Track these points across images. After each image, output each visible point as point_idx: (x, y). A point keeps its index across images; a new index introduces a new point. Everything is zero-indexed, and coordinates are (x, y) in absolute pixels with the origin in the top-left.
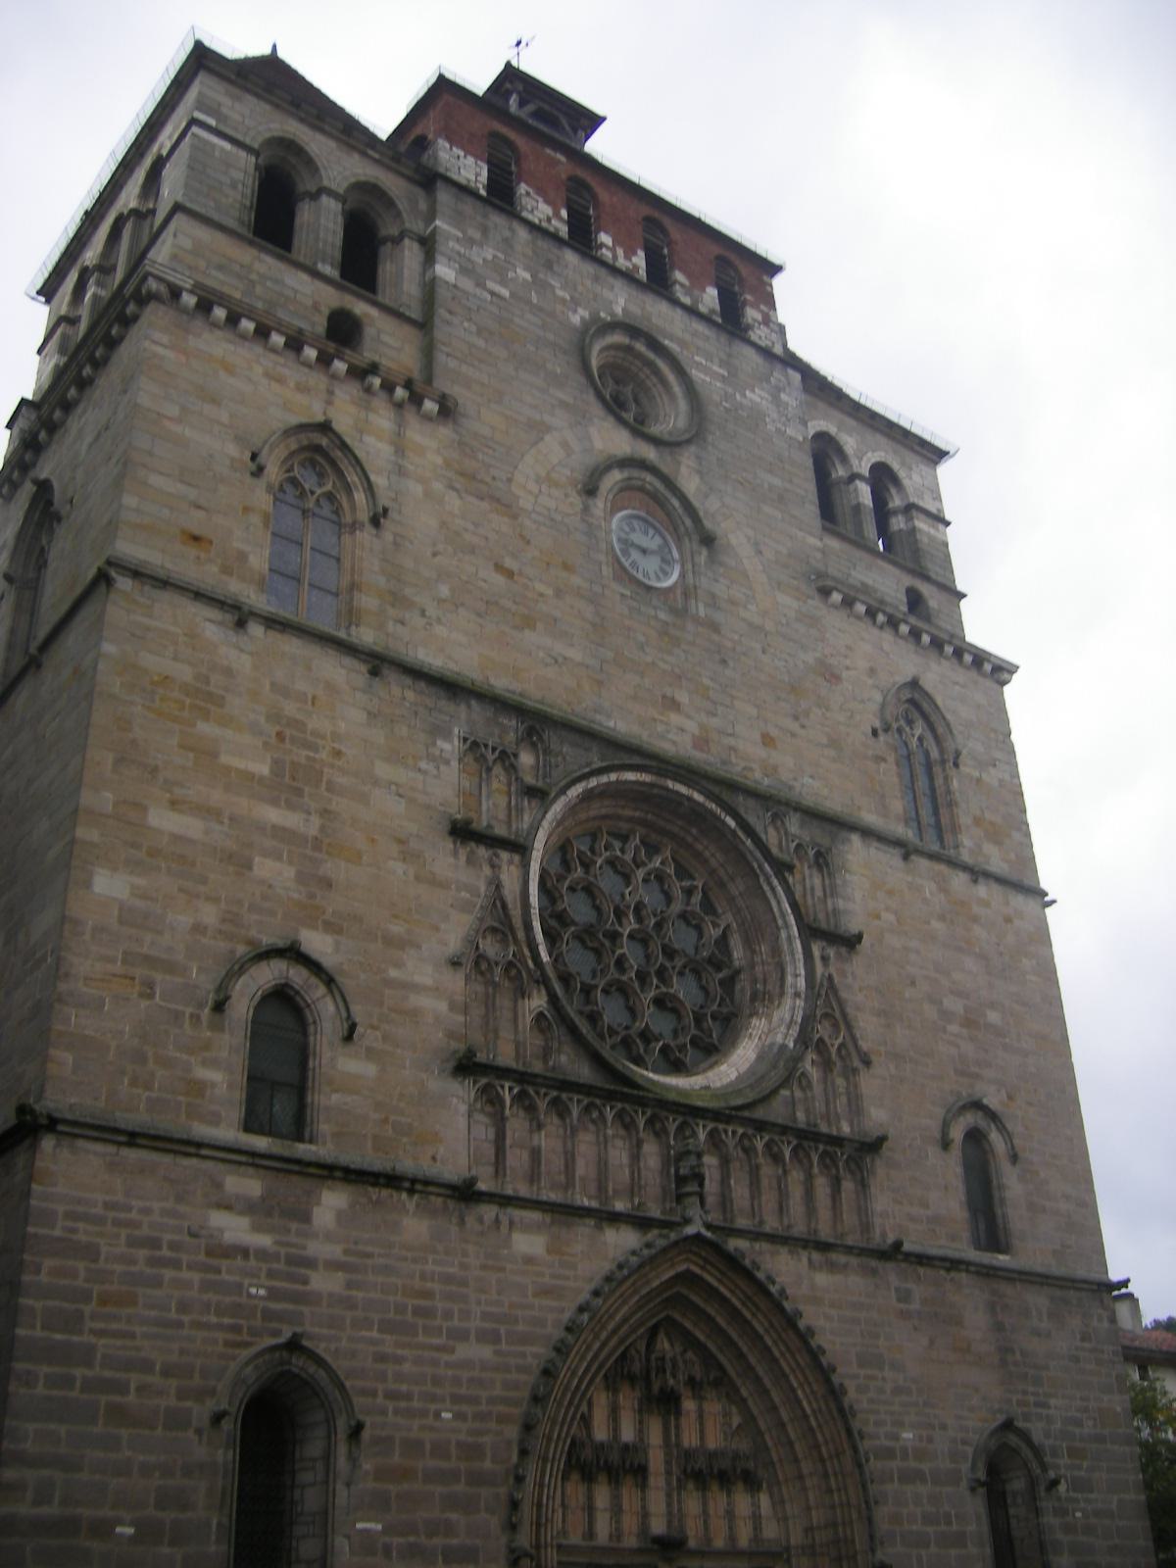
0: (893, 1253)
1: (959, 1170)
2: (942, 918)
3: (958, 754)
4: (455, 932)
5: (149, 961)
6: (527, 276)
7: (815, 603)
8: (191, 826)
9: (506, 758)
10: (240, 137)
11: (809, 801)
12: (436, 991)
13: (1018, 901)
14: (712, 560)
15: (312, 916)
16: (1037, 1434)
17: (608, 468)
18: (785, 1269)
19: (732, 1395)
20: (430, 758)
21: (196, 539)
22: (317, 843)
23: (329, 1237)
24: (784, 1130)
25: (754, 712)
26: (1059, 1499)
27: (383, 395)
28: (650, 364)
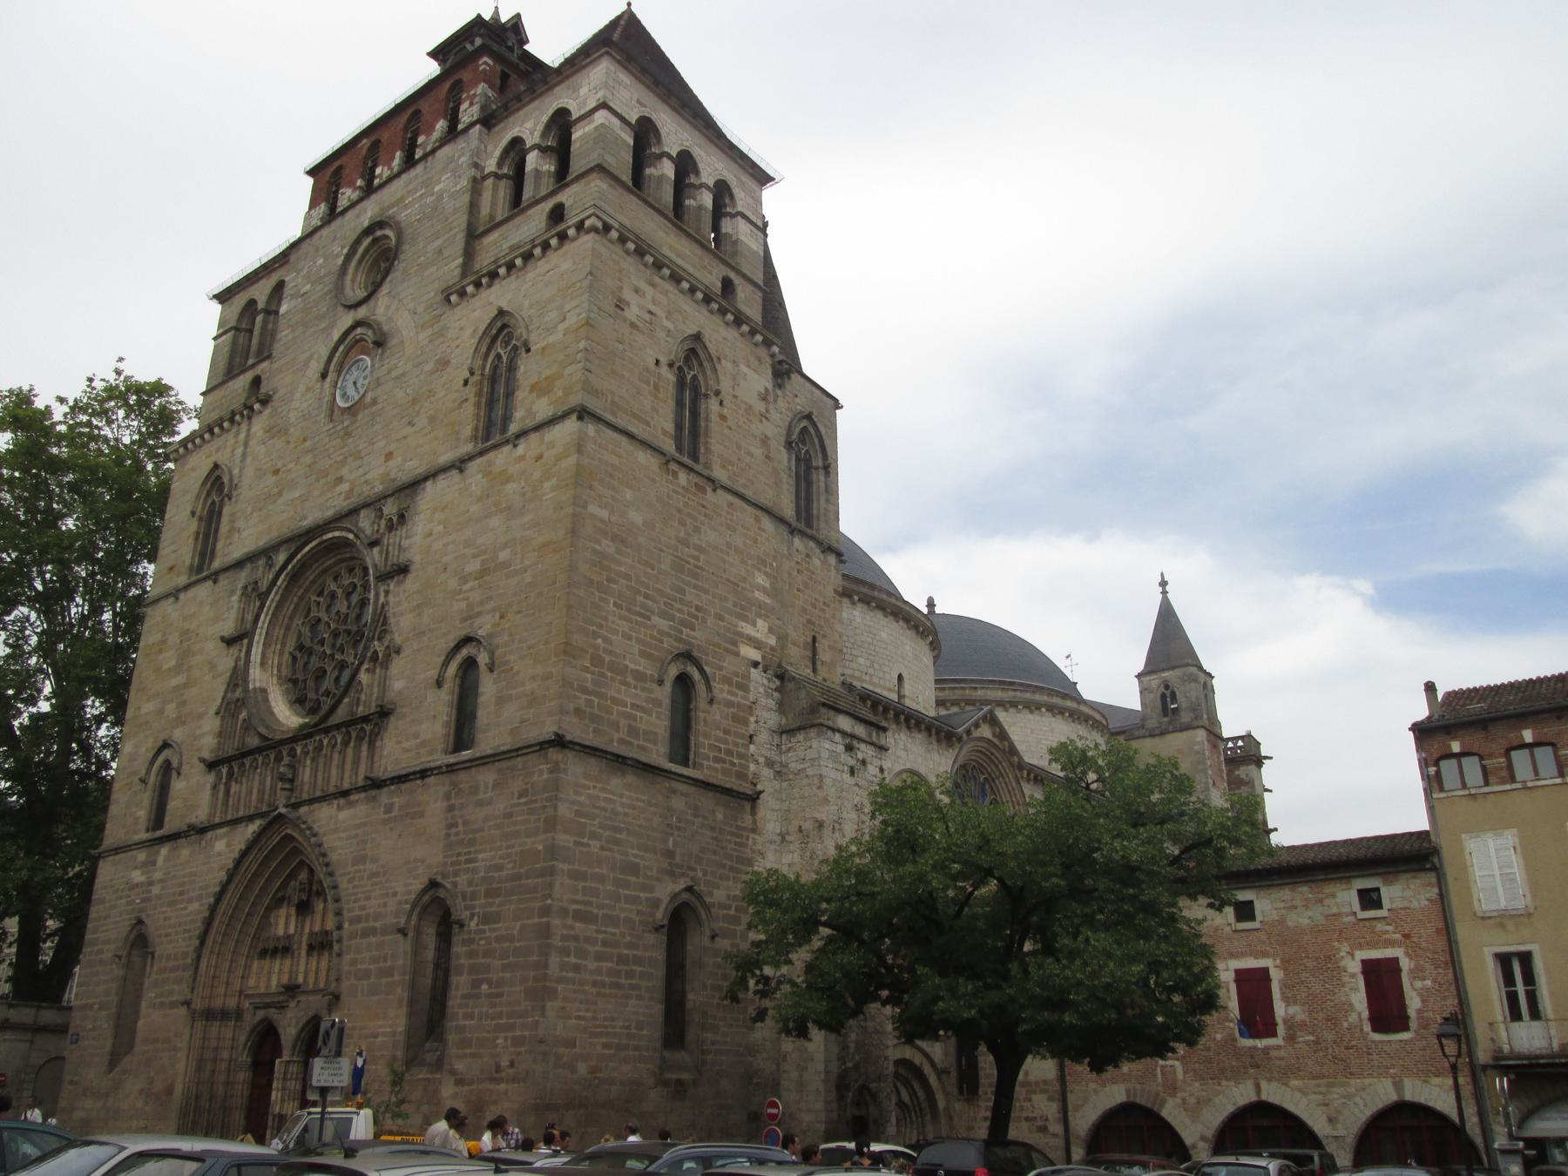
0: (375, 784)
2: (480, 499)
15: (180, 721)
16: (462, 880)
26: (469, 932)
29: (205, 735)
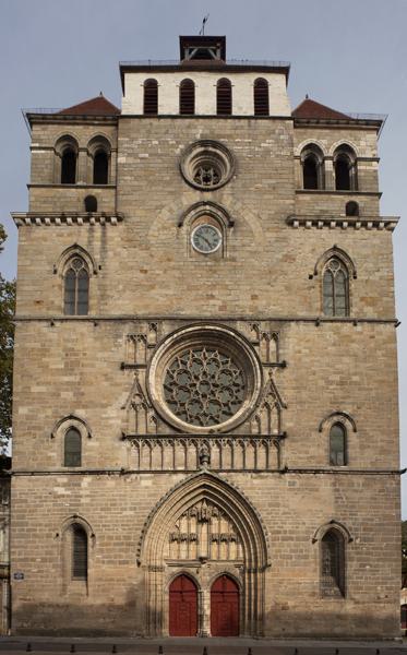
1: (327, 438)
2: (334, 345)
3: (355, 273)
4: (123, 398)
5: (34, 428)
6: (157, 142)
7: (289, 230)
8: (43, 389)
9: (143, 337)
10: (47, 145)
11: (271, 316)
12: (118, 417)
13: (389, 327)
14: (234, 232)
15: (78, 405)
16: (349, 524)
17: (189, 211)
18: (240, 481)
19: (230, 520)
20: (116, 346)
21: (38, 302)
22: (79, 384)
23: (86, 489)
24: (244, 437)
25: (248, 288)
27: (98, 224)
28: (216, 154)
29: (115, 416)
